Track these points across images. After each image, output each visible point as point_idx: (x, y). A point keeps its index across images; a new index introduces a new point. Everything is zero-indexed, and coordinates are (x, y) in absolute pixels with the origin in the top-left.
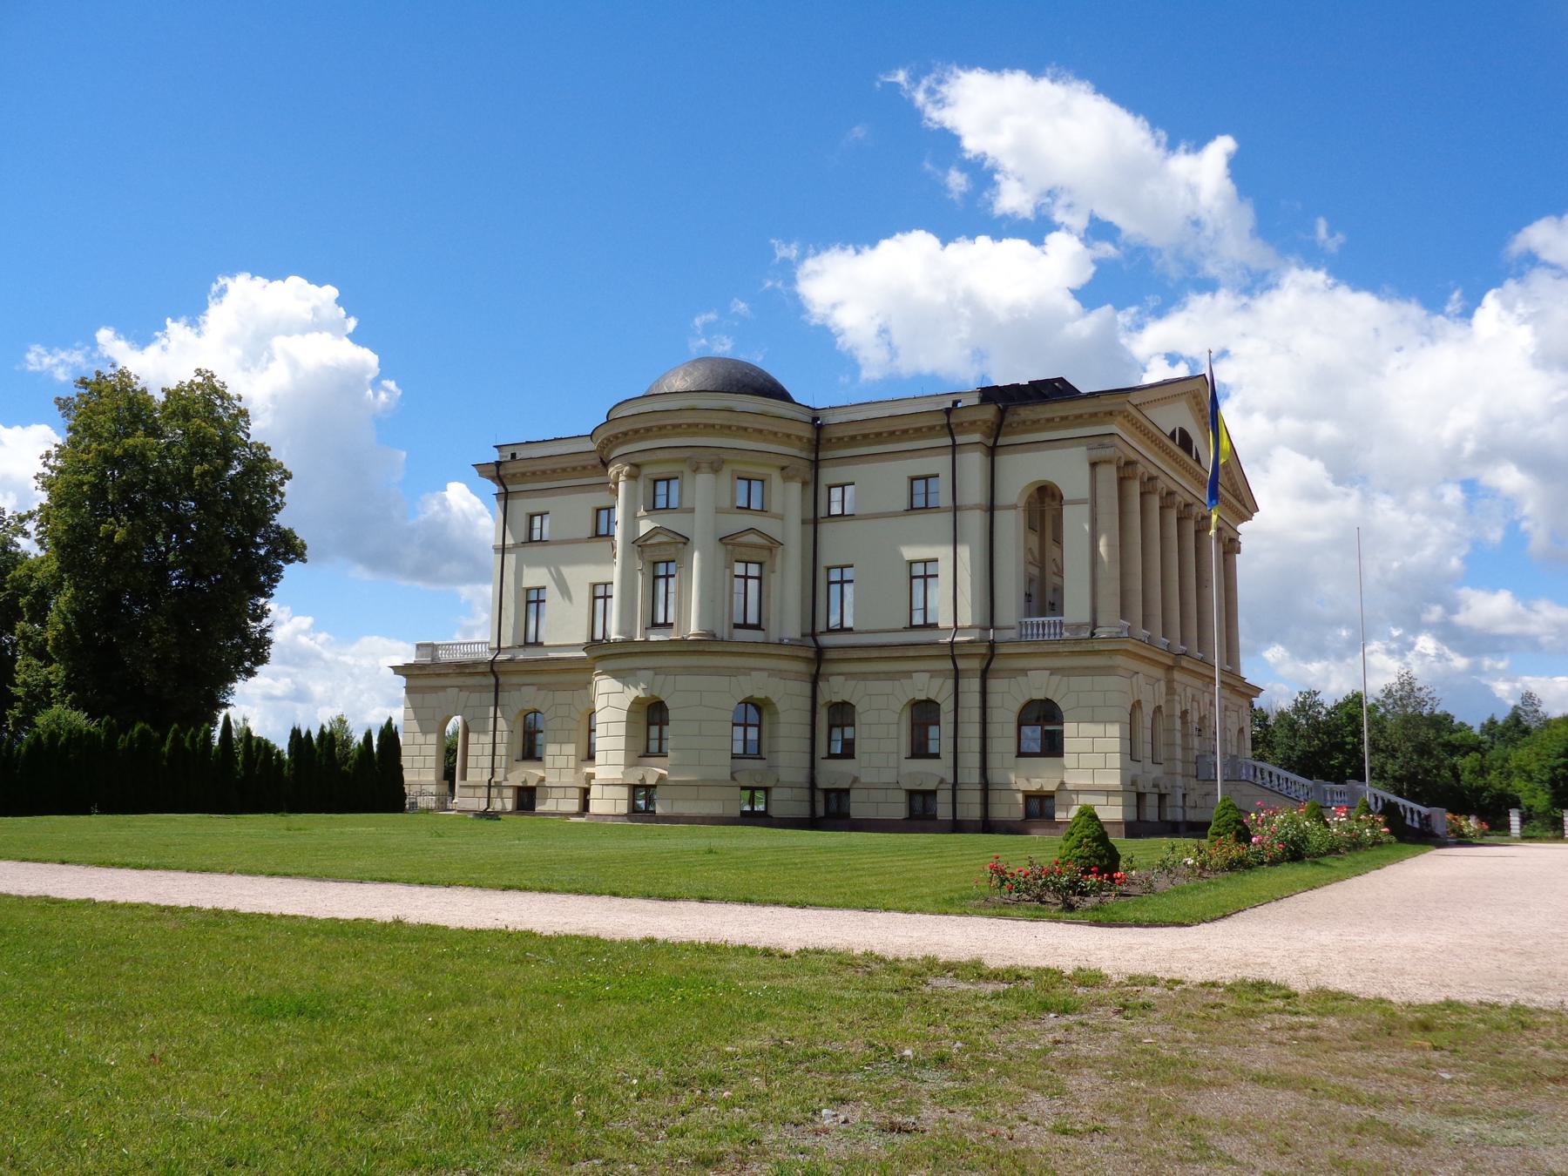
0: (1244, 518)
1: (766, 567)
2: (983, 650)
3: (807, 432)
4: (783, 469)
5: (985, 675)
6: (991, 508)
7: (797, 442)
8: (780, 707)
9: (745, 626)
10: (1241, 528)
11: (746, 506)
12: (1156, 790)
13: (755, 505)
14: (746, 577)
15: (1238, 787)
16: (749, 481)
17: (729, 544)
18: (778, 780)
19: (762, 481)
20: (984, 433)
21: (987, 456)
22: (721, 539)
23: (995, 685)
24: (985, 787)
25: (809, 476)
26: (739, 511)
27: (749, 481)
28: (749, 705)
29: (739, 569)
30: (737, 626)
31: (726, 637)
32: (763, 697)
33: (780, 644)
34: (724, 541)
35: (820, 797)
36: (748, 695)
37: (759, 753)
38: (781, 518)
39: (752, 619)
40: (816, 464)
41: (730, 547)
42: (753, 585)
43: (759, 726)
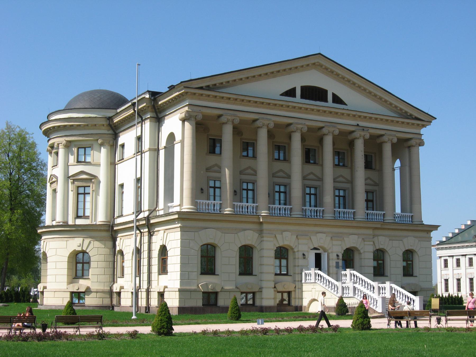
0: (424, 126)
2: (144, 222)
3: (105, 123)
5: (150, 235)
6: (155, 151)
7: (103, 127)
9: (84, 217)
10: (423, 131)
12: (238, 290)
14: (85, 194)
15: (315, 287)
16: (85, 148)
19: (90, 147)
20: (152, 112)
21: (156, 122)
23: (154, 238)
24: (148, 292)
25: (111, 143)
27: (85, 148)
31: (70, 223)
35: (115, 296)
40: (116, 136)
41: (72, 180)
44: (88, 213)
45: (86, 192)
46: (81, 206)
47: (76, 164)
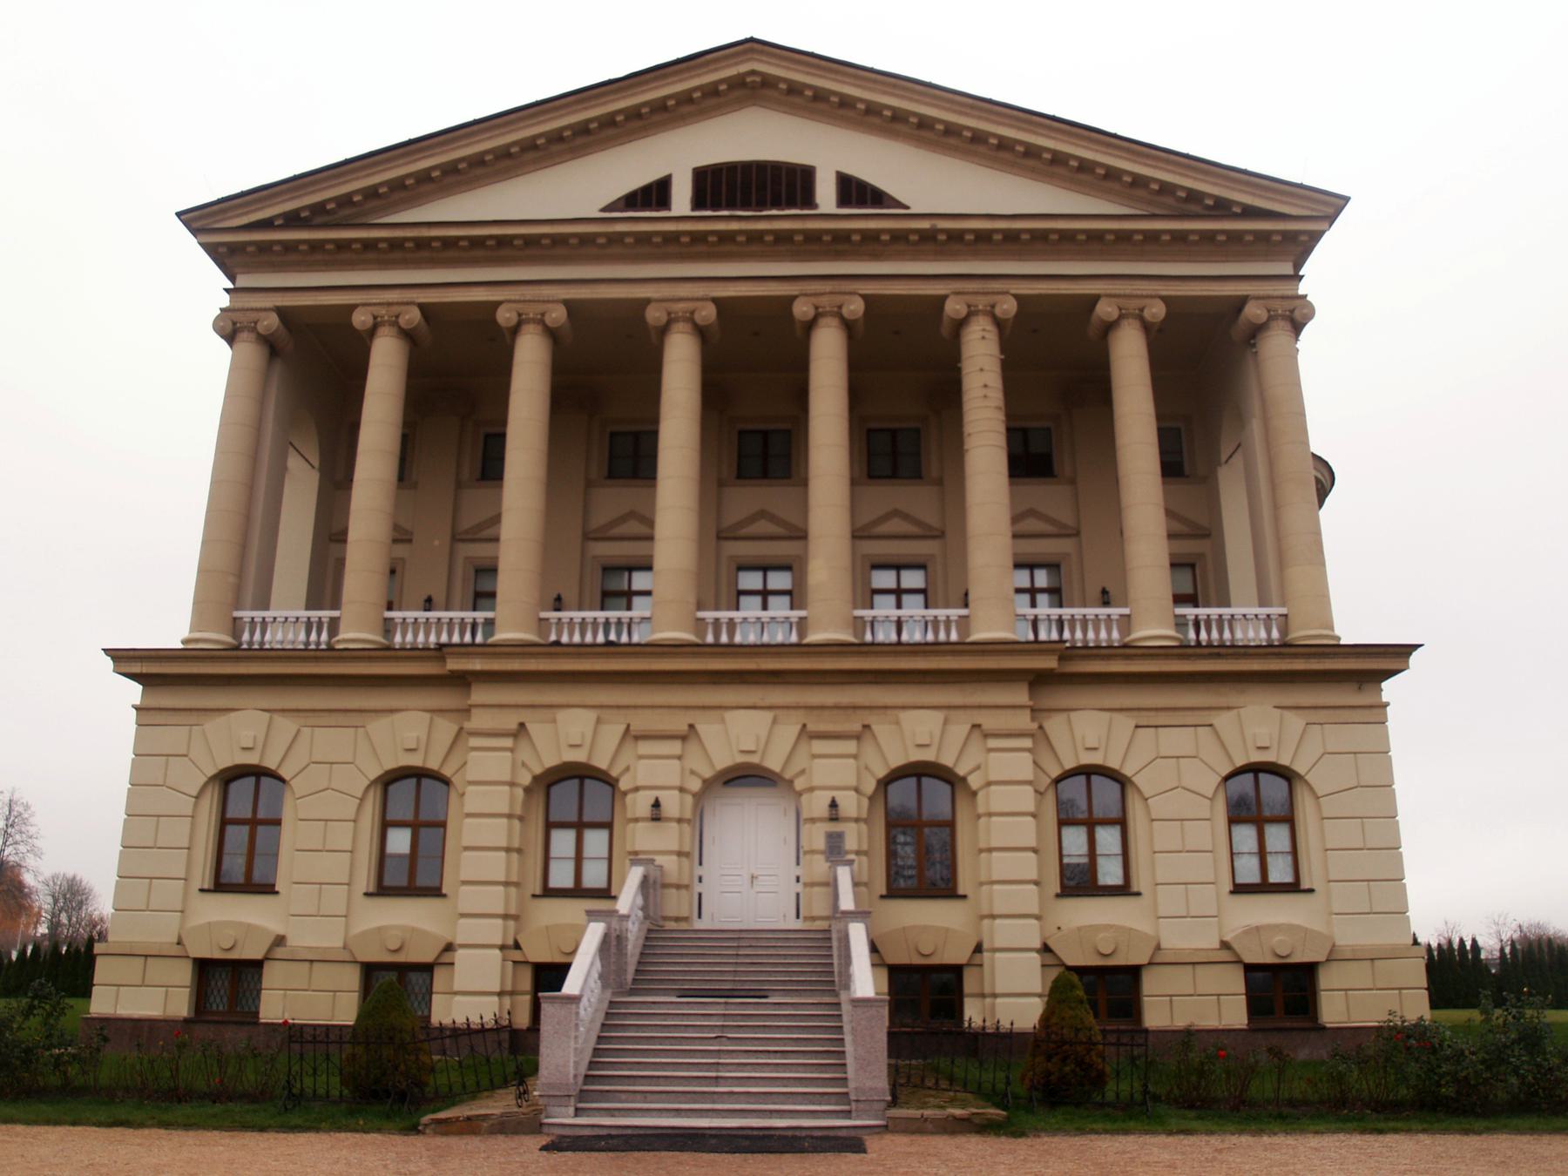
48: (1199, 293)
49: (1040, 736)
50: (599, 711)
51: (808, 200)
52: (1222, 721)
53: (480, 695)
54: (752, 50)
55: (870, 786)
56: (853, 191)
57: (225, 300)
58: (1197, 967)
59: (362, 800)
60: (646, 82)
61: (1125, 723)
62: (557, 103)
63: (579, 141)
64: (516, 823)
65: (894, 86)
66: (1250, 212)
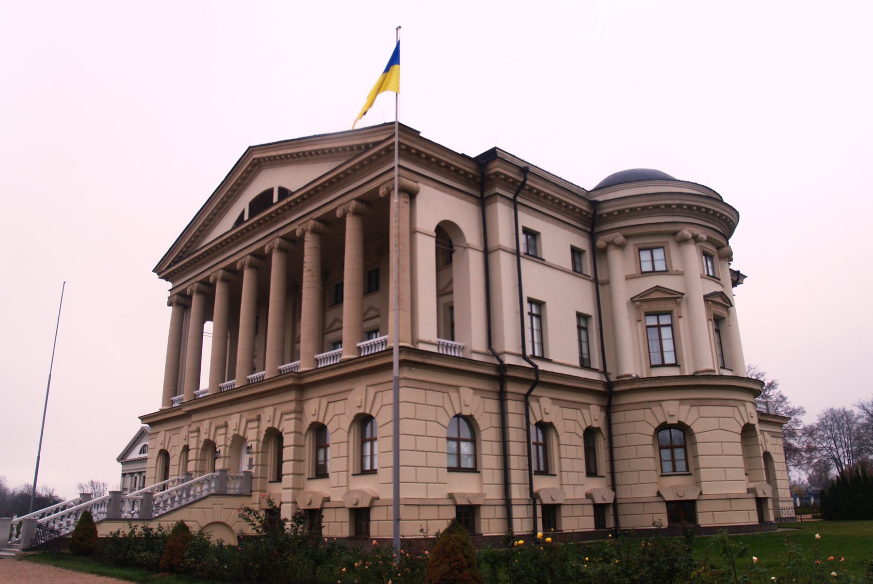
1: (675, 314)
4: (674, 234)
8: (695, 428)
9: (663, 365)
11: (650, 269)
13: (660, 266)
14: (659, 326)
17: (636, 301)
18: (701, 494)
22: (631, 299)
26: (642, 275)
27: (651, 249)
28: (672, 430)
29: (652, 321)
30: (652, 366)
31: (645, 376)
32: (677, 422)
33: (694, 376)
34: (634, 300)
36: (662, 421)
37: (688, 469)
38: (681, 274)
39: (669, 358)
42: (666, 333)
43: (684, 447)
44: (669, 358)
45: (661, 323)
46: (655, 346)
47: (640, 275)
48: (367, 191)
49: (299, 412)
50: (211, 420)
51: (271, 204)
52: (350, 396)
53: (195, 418)
54: (252, 151)
55: (262, 438)
56: (284, 193)
57: (169, 294)
58: (337, 509)
59: (180, 457)
60: (231, 177)
61: (324, 401)
62: (213, 197)
63: (226, 205)
64: (199, 462)
65: (281, 146)
66: (376, 144)
